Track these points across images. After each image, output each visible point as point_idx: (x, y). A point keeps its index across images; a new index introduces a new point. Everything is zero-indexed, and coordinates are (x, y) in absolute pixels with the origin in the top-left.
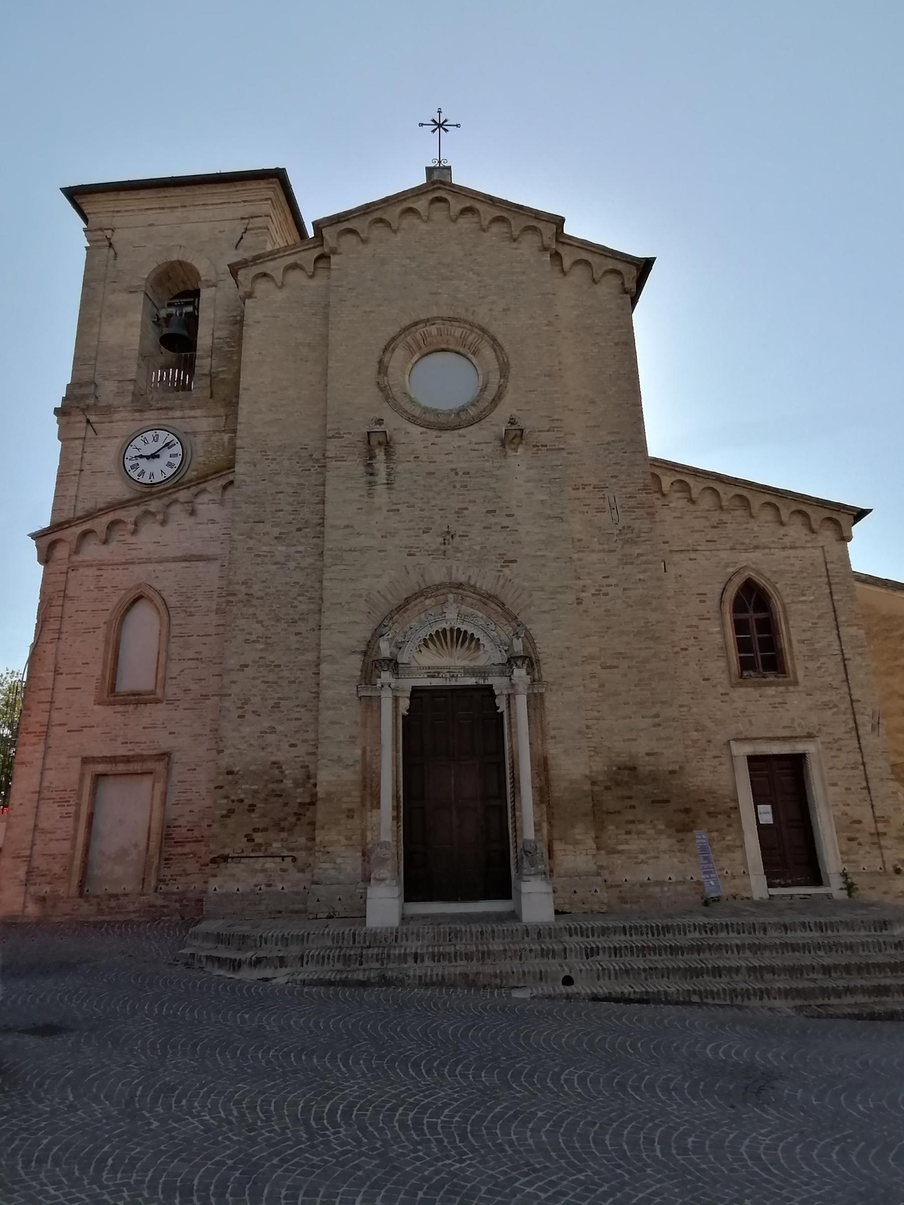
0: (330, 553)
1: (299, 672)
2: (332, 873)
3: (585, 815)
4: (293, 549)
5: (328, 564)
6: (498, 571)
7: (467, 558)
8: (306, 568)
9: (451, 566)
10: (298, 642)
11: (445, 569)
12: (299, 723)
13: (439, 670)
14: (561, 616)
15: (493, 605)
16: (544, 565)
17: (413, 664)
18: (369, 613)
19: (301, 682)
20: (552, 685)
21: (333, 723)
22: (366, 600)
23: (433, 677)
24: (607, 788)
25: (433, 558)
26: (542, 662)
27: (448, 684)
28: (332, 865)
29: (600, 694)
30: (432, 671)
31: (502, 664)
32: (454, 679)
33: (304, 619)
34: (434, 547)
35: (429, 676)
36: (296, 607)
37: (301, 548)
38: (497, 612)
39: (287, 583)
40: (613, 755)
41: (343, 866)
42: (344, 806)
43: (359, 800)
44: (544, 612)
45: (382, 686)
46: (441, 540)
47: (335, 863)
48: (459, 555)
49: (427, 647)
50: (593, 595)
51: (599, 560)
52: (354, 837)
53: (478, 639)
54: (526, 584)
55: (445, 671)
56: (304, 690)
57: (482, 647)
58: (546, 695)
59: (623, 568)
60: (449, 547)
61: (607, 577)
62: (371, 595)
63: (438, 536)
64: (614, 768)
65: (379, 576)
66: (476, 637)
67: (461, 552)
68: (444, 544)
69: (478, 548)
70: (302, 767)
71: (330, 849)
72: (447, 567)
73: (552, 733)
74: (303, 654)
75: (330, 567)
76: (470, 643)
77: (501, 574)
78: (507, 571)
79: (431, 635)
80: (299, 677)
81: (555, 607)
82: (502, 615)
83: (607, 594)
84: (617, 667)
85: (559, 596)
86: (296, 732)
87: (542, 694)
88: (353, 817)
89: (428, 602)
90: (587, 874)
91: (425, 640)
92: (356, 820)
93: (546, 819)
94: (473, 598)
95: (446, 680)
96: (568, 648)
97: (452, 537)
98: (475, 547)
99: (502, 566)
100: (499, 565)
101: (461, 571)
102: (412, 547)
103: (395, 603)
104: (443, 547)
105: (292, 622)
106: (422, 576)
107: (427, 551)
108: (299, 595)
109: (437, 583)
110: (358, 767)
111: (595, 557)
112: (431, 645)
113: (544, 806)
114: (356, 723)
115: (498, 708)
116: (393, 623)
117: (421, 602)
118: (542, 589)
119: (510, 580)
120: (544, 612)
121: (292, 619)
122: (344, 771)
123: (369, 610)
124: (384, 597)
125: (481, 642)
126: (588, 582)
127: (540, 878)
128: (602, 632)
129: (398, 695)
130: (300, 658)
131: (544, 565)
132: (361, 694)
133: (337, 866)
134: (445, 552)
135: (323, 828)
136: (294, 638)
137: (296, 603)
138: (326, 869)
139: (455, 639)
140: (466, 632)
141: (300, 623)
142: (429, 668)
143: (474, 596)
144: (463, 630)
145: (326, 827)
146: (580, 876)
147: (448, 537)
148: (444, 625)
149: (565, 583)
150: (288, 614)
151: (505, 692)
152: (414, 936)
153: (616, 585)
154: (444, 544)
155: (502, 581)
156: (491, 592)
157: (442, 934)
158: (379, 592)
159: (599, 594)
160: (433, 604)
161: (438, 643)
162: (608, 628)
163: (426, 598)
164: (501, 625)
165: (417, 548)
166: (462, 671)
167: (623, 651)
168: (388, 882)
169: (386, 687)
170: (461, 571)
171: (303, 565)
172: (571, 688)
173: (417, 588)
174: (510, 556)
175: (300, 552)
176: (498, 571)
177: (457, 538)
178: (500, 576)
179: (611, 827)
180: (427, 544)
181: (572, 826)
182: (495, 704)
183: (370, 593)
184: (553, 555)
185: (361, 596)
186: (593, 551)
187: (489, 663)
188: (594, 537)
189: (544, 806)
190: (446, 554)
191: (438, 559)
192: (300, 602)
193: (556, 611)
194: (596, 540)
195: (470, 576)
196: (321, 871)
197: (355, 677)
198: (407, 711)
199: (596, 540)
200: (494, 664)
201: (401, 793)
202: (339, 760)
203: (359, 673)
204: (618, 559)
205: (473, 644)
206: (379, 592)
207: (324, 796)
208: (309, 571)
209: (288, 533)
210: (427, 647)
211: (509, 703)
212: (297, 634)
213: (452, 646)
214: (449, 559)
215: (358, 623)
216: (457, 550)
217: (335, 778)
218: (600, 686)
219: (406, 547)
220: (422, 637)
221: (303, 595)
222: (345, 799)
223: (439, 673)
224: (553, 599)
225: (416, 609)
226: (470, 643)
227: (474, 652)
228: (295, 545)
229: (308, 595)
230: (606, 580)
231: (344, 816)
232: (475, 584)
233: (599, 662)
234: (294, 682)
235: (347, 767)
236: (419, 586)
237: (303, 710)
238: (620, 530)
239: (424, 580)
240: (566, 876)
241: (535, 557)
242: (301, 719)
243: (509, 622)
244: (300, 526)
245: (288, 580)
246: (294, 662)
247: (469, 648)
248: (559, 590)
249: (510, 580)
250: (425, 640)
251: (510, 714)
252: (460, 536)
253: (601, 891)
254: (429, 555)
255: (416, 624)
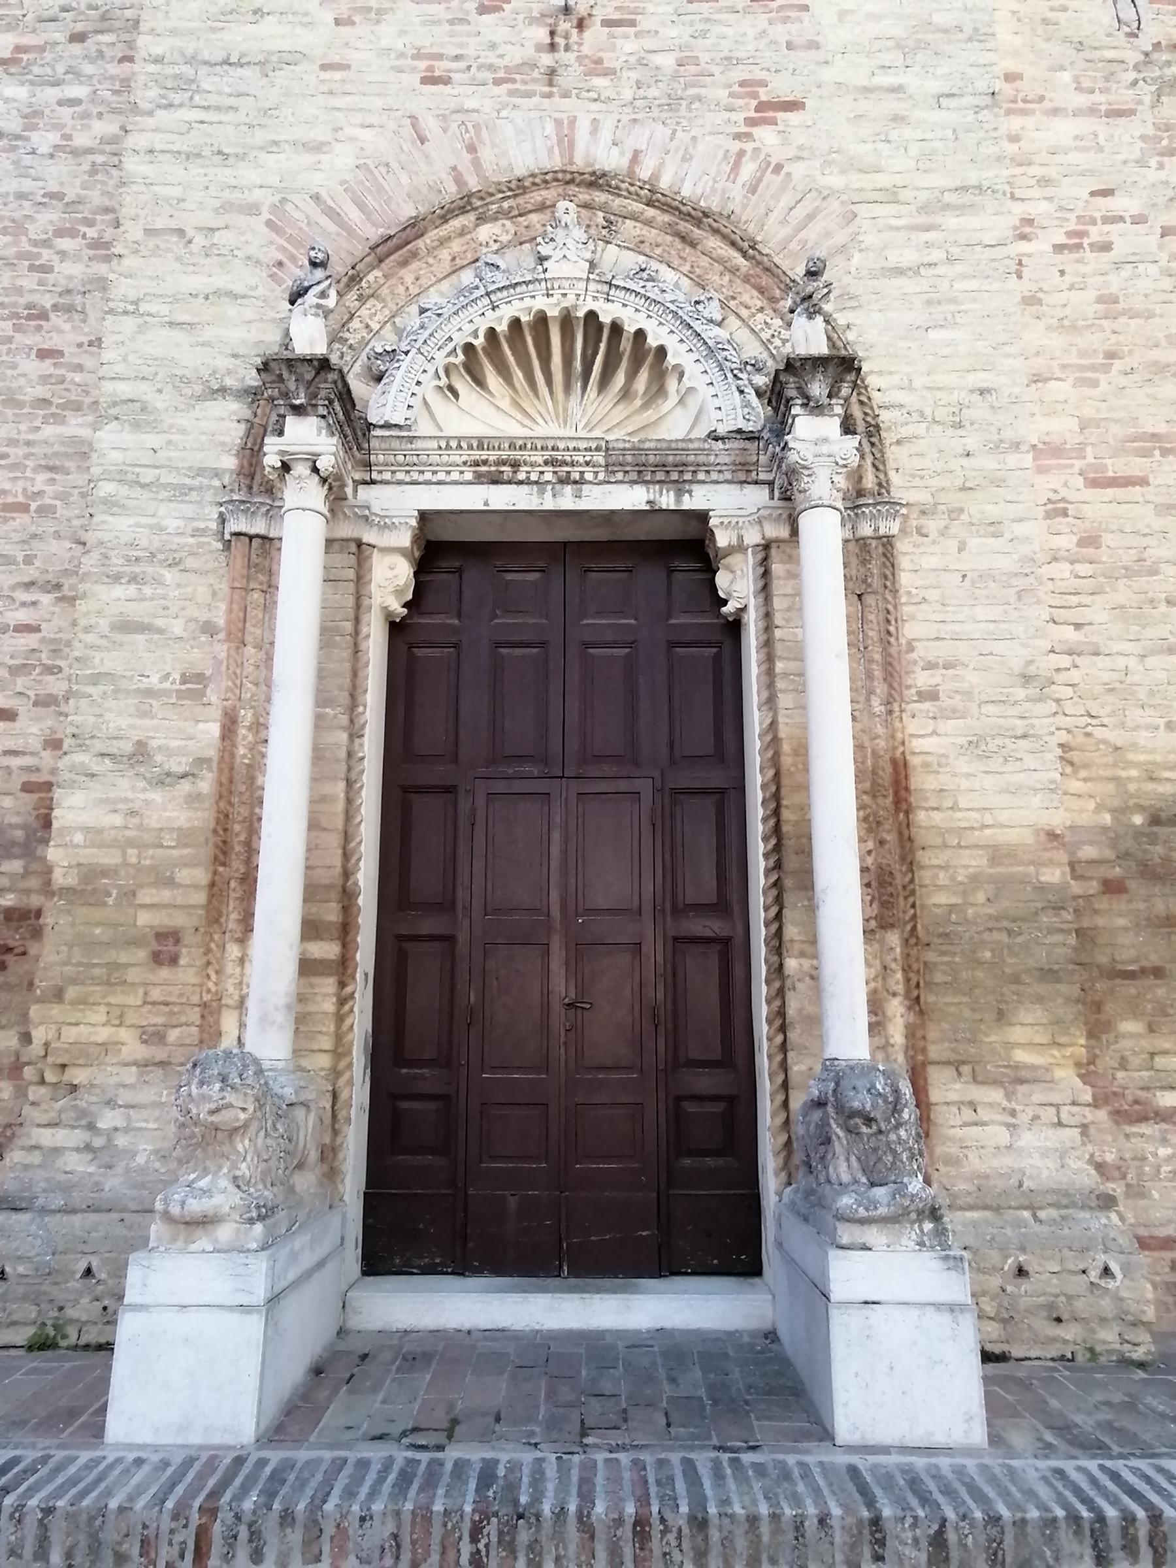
0: (151, 68)
1: (41, 477)
2: (77, 1164)
3: (1048, 974)
4: (51, 94)
5: (144, 105)
6: (738, 136)
7: (628, 94)
8: (89, 151)
9: (573, 121)
10: (44, 379)
11: (550, 128)
12: (29, 641)
13: (516, 455)
14: (958, 286)
15: (713, 243)
16: (898, 119)
17: (424, 428)
18: (280, 264)
19: (44, 511)
20: (923, 513)
21: (127, 626)
22: (269, 224)
23: (496, 481)
24: (1112, 887)
25: (511, 93)
26: (888, 437)
27: (549, 504)
28: (78, 1137)
29: (1084, 569)
30: (493, 456)
31: (751, 437)
32: (568, 489)
33: (69, 309)
34: (515, 55)
35: (479, 479)
36: (46, 269)
37: (77, 91)
38: (734, 271)
39: (21, 196)
40: (1134, 773)
41: (121, 1141)
42: (144, 919)
43: (200, 898)
44: (899, 271)
45: (286, 467)
46: (541, 34)
47: (91, 1127)
48: (600, 82)
49: (479, 382)
50: (1059, 248)
51: (1076, 138)
52: (173, 1035)
53: (661, 351)
54: (835, 180)
55: (538, 457)
56: (57, 535)
57: (672, 384)
58: (901, 546)
59: (1161, 166)
60: (569, 57)
61: (1106, 193)
62: (289, 207)
63: (532, 21)
64: (1138, 820)
65: (319, 147)
66: (652, 342)
67: (610, 73)
68: (553, 47)
69: (667, 61)
70: (28, 788)
71: (78, 1076)
72: (558, 123)
73: (922, 679)
74: (59, 420)
75: (150, 113)
76: (632, 375)
77: (749, 146)
78: (766, 136)
79: (492, 333)
80: (40, 493)
81: (937, 255)
82: (746, 279)
83: (1106, 247)
84: (1143, 482)
85: (951, 221)
86: (15, 671)
87: (887, 542)
88: (174, 960)
89: (485, 232)
90: (1065, 1199)
91: (469, 348)
92: (186, 974)
93: (900, 988)
94: (648, 223)
95: (542, 492)
96: (982, 392)
97: (581, 25)
98: (658, 59)
99: (751, 122)
100: (739, 117)
101: (606, 135)
102: (440, 57)
103: (374, 233)
104: (546, 60)
105: (30, 317)
106: (472, 149)
107: (491, 67)
108: (60, 233)
109: (520, 172)
110: (206, 784)
111: (1064, 129)
112: (492, 379)
113: (894, 939)
114: (208, 629)
115: (725, 602)
116: (362, 299)
117: (462, 233)
118: (891, 196)
119: (778, 168)
120: (899, 271)
121: (30, 306)
122: (156, 796)
123: (280, 256)
124: (330, 213)
125: (671, 360)
126: (1039, 208)
127: (909, 1236)
128: (1093, 368)
129: (369, 537)
130: (49, 431)
131: (898, 119)
132: (233, 526)
133: (98, 1142)
134: (552, 73)
135: (58, 995)
136: (33, 367)
137: (46, 255)
138: (57, 1151)
139: (578, 364)
140: (616, 329)
141: (56, 319)
142: (480, 447)
143: (651, 212)
144: (605, 319)
145: (71, 992)
146: (1032, 1208)
147: (564, 25)
148: (541, 303)
149: (973, 178)
150: (19, 291)
151: (753, 537)
152: (295, 1537)
153: (1139, 220)
154: (553, 47)
155: (748, 170)
156: (713, 203)
157: (437, 1531)
158: (316, 198)
159: (1079, 246)
160: (505, 238)
161: (518, 375)
162: (1111, 355)
163: (482, 219)
164: (744, 313)
165: (457, 58)
166: (600, 458)
167: (1162, 428)
168: (225, 1233)
169: (301, 469)
170: (606, 135)
171: (81, 140)
172: (994, 527)
173: (452, 188)
174: (781, 87)
175: (73, 102)
176: (738, 136)
177: (595, 33)
178: (741, 153)
179: (1129, 1026)
180: (493, 46)
181: (1001, 1017)
182: (714, 588)
183: (284, 200)
184: (934, 86)
185: (253, 209)
186: (1055, 112)
187: (701, 432)
188: (1062, 68)
189: (894, 939)
190: (558, 80)
191: (529, 95)
192: (63, 254)
193: (939, 270)
194: (1066, 77)
195: (636, 154)
196: (36, 1158)
197: (217, 474)
198: (405, 606)
199: (1066, 77)
200: (714, 436)
201: (367, 876)
202: (141, 753)
203: (230, 462)
204: (1143, 138)
205: (643, 377)
206: (316, 198)
207: (72, 881)
208: (100, 159)
209: (41, 49)
210: (479, 382)
211: (766, 574)
212: (43, 354)
213: (568, 388)
214: (566, 95)
215: (234, 296)
216: (597, 67)
217: (118, 820)
218: (1083, 542)
219: (418, 56)
220: (460, 339)
221: (72, 233)
222: (147, 896)
223: (515, 465)
224: (928, 228)
225: (445, 254)
226: (632, 375)
227: (646, 406)
228: (56, 84)
229: (91, 233)
230: (1100, 200)
231: (142, 954)
232: (656, 176)
233: (1078, 464)
234: (24, 508)
235: (166, 779)
236: (459, 180)
237: (46, 599)
238: (1147, 54)
239: (476, 163)
240: (986, 1208)
241: (867, 90)
242: (37, 629)
243: (773, 300)
244: (79, 27)
245: (27, 185)
246: (28, 443)
247: (626, 394)
248: (948, 198)
249: (778, 168)
250: (469, 348)
251: (768, 615)
252: (607, 23)
253: (1127, 1270)
254: (497, 82)
255: (442, 301)
